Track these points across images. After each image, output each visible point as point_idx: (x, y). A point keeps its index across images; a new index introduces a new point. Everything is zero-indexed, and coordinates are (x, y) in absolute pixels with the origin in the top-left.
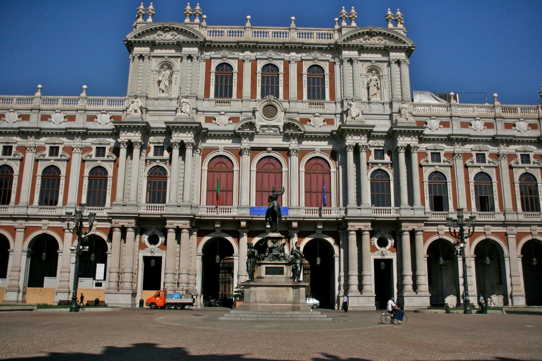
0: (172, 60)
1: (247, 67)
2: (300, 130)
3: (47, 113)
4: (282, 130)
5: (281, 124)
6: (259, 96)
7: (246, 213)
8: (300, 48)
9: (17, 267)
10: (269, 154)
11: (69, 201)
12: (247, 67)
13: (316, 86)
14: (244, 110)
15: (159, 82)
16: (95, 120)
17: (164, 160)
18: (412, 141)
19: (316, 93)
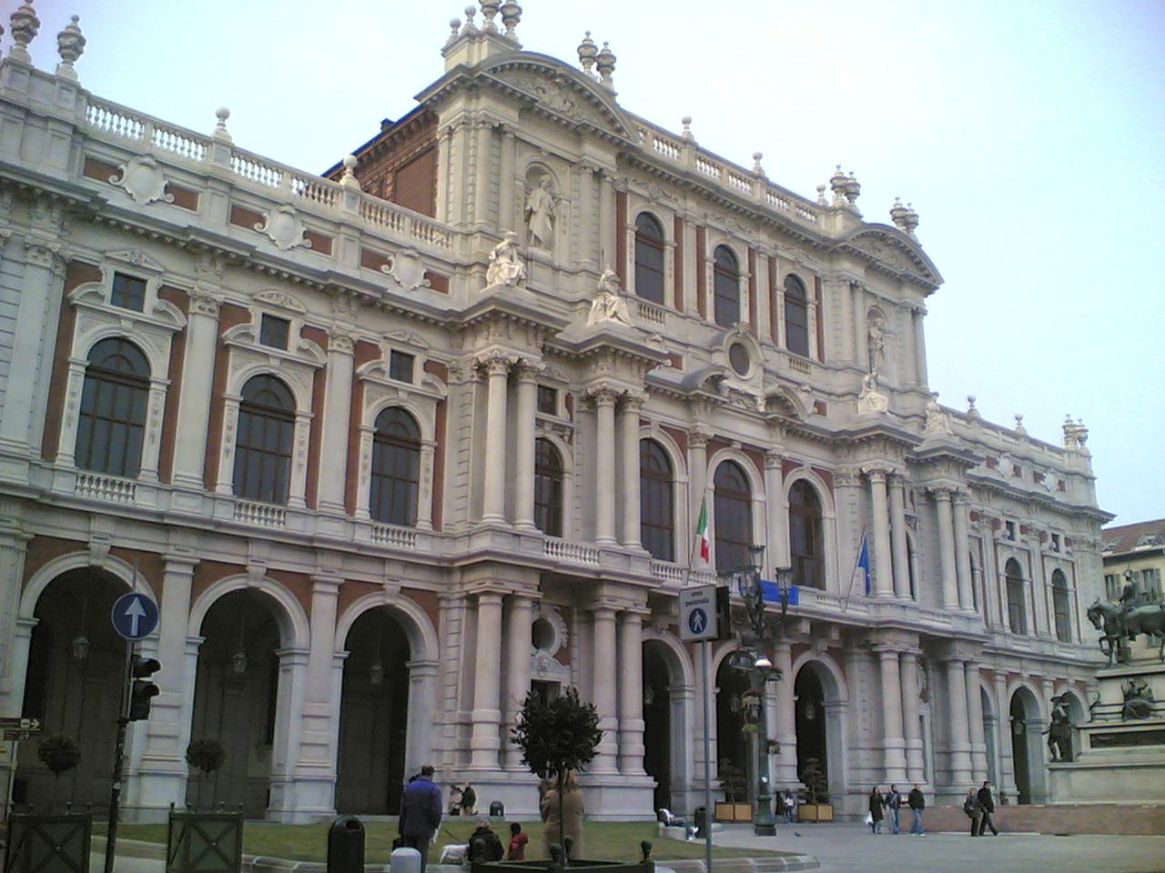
1: (689, 236)
3: (252, 205)
4: (762, 409)
5: (759, 393)
6: (710, 318)
8: (779, 229)
12: (689, 236)
16: (384, 267)
17: (558, 427)
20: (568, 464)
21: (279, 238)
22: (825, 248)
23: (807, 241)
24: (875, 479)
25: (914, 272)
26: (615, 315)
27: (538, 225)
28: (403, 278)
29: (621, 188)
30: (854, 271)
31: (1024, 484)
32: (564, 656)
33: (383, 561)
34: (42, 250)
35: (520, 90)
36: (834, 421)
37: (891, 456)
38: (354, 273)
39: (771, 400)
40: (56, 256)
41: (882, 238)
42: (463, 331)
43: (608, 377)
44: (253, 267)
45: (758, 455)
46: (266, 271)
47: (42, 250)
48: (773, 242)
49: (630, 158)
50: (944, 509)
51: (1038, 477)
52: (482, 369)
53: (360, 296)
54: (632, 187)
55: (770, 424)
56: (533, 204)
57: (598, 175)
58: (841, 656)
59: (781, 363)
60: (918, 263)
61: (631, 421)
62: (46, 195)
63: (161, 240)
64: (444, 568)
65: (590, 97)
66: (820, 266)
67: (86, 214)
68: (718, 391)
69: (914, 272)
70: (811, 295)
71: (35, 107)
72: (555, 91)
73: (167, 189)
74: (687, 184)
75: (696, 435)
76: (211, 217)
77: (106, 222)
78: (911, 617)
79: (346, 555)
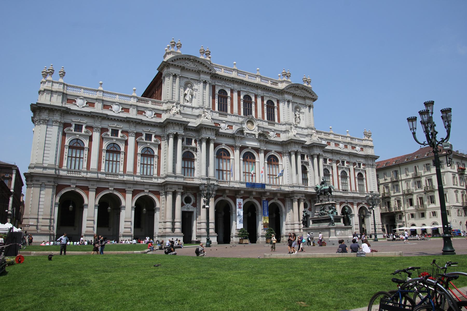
0: (192, 81)
2: (267, 139)
4: (257, 137)
5: (257, 133)
7: (244, 186)
8: (264, 88)
9: (92, 217)
10: (249, 151)
11: (127, 170)
13: (222, 103)
14: (236, 121)
15: (185, 95)
16: (144, 114)
18: (211, 135)
19: (271, 117)
20: (196, 157)
21: (116, 111)
22: (279, 92)
23: (273, 91)
24: (292, 153)
25: (309, 96)
26: (207, 118)
27: (187, 98)
28: (149, 116)
29: (214, 84)
30: (290, 97)
31: (349, 150)
32: (195, 205)
33: (144, 185)
34: (56, 122)
35: (180, 64)
36: (283, 138)
37: (297, 146)
38: (135, 117)
39: (260, 135)
40: (60, 123)
41: (298, 87)
42: (164, 127)
43: (206, 135)
44: (108, 119)
45: (258, 150)
46: (111, 119)
47: (56, 122)
48: (262, 92)
49: (215, 76)
50: (316, 160)
51: (353, 148)
52: (168, 136)
53: (135, 122)
54: (216, 83)
55: (260, 141)
56: (186, 92)
57: (205, 82)
58: (283, 201)
59: (266, 125)
60: (310, 93)
61: (212, 146)
62: (56, 109)
63: (85, 115)
64: (159, 185)
65: (201, 63)
66: (278, 97)
67: (66, 112)
68: (243, 134)
69: (309, 96)
70: (276, 105)
71: (53, 90)
72: (191, 63)
73: (87, 103)
74: (234, 81)
75: (236, 146)
76: (98, 108)
77: (71, 113)
78: (302, 189)
79: (134, 184)
